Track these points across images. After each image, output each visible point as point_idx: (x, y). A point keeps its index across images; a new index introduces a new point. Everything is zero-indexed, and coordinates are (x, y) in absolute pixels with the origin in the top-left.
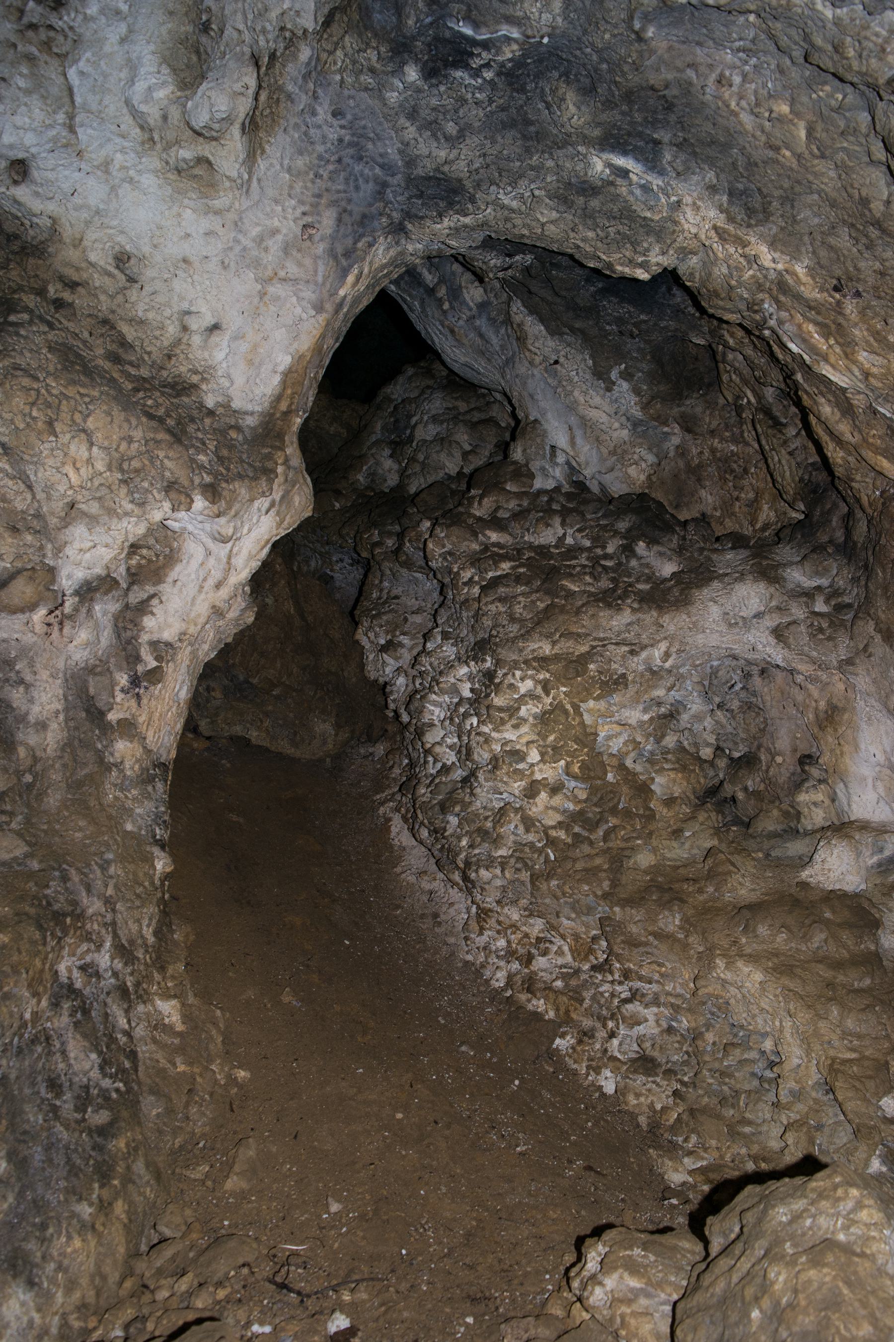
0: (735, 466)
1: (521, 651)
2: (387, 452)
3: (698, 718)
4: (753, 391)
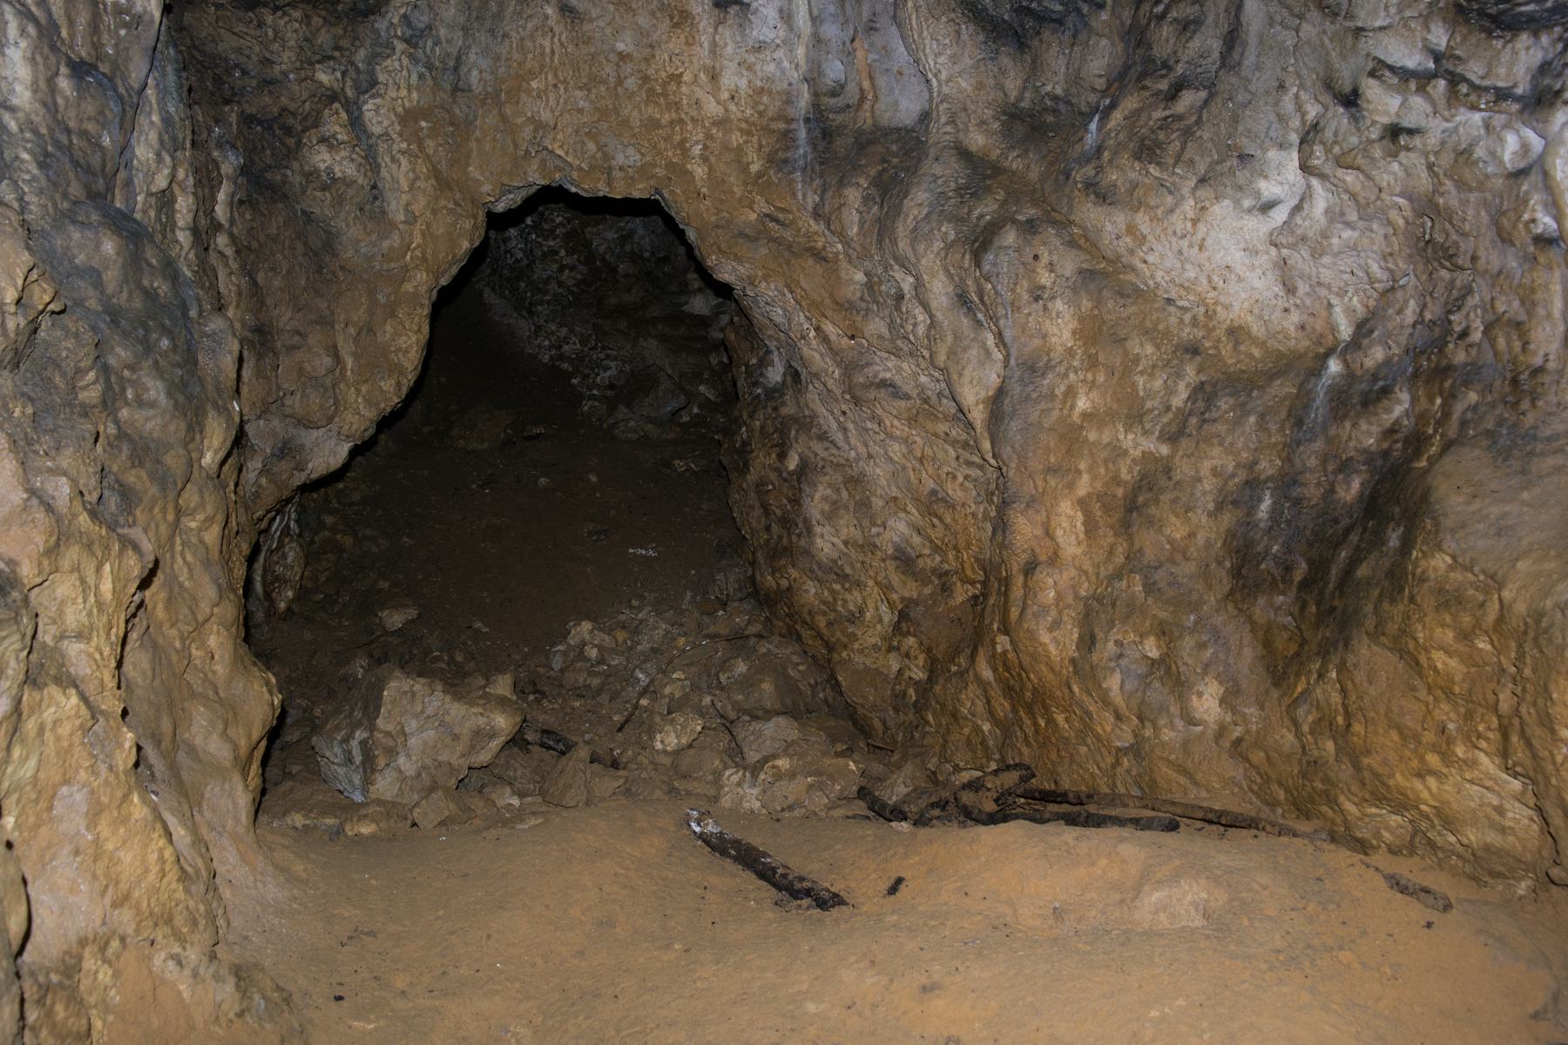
3: (643, 237)
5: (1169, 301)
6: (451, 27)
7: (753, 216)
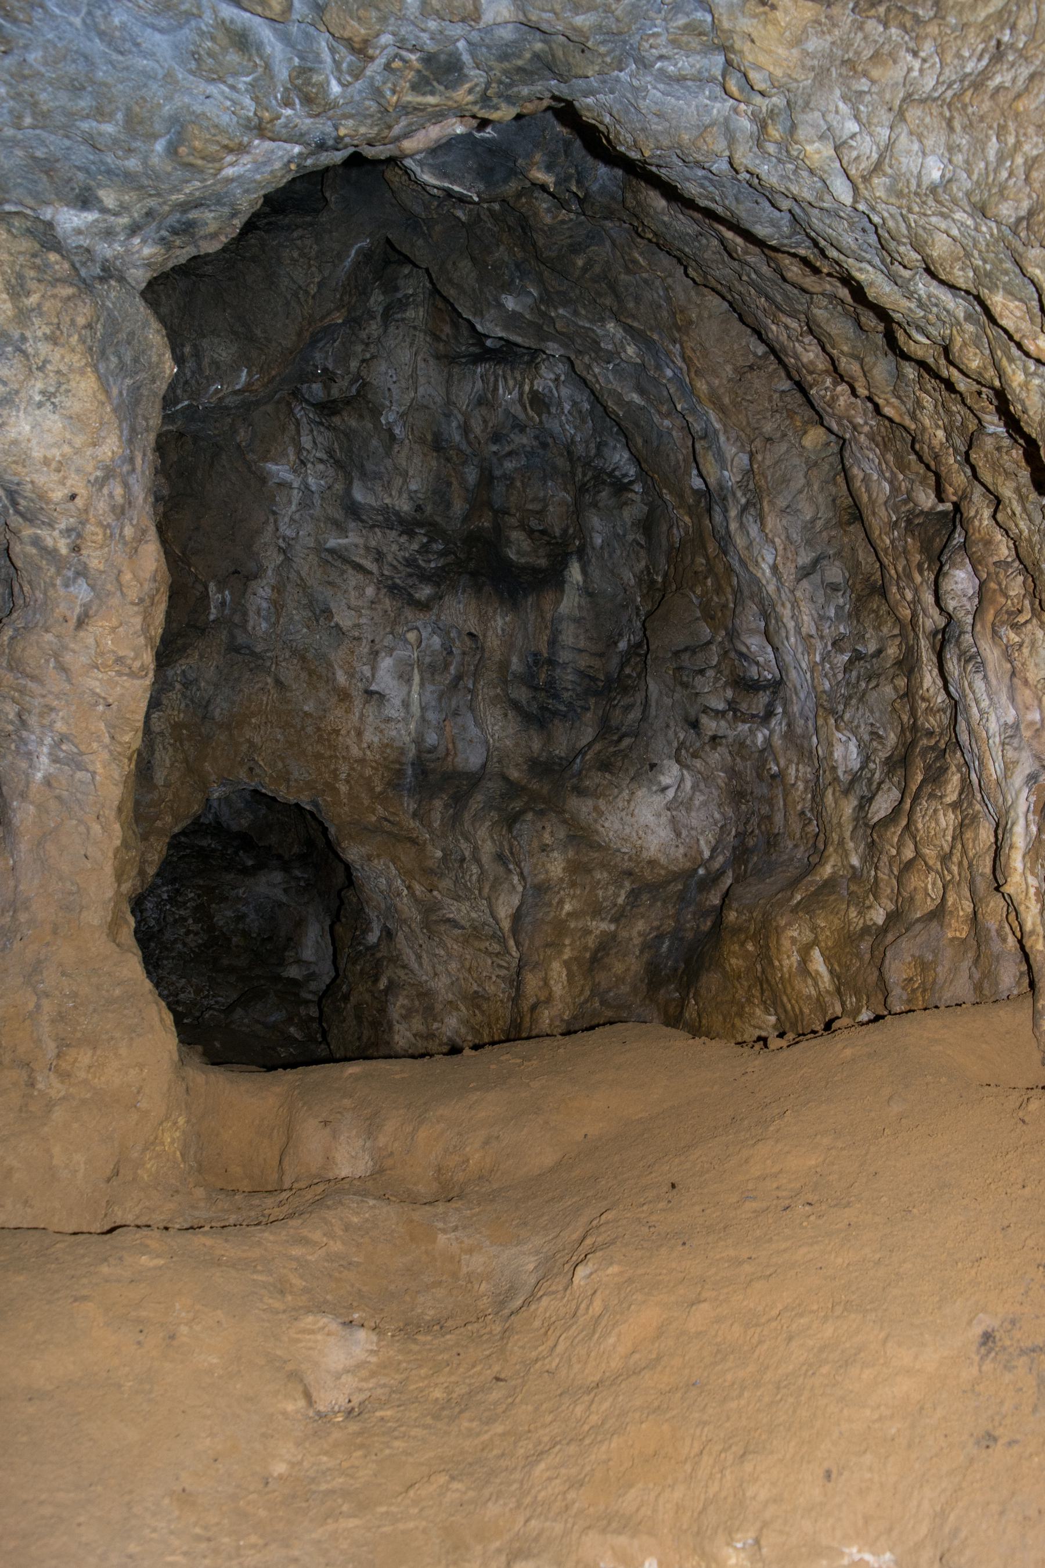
5: (618, 850)
6: (208, 683)
7: (374, 819)
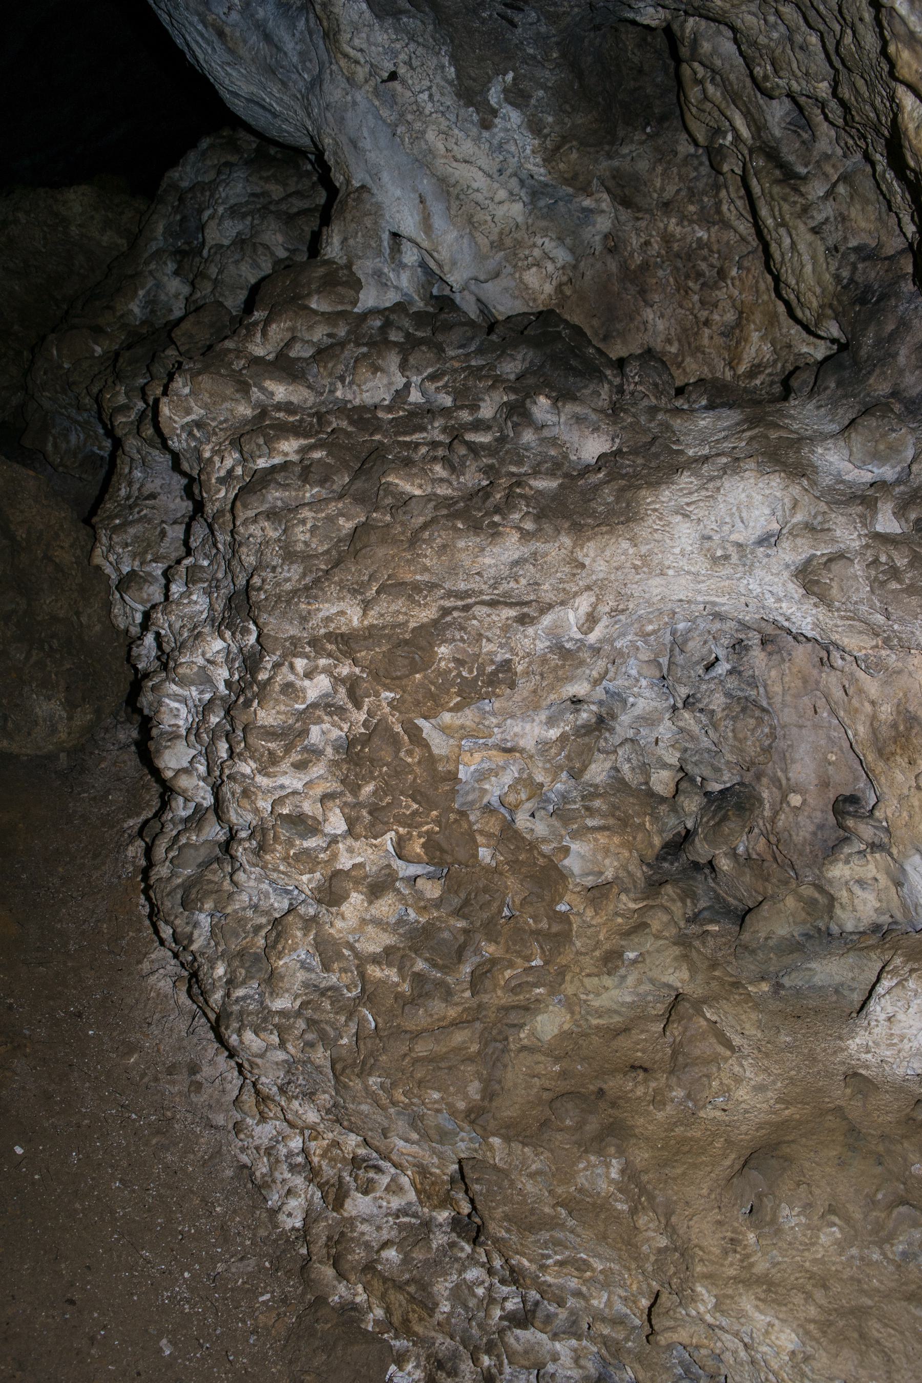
0: (703, 266)
1: (304, 619)
2: (171, 266)
3: (649, 720)
4: (747, 115)
